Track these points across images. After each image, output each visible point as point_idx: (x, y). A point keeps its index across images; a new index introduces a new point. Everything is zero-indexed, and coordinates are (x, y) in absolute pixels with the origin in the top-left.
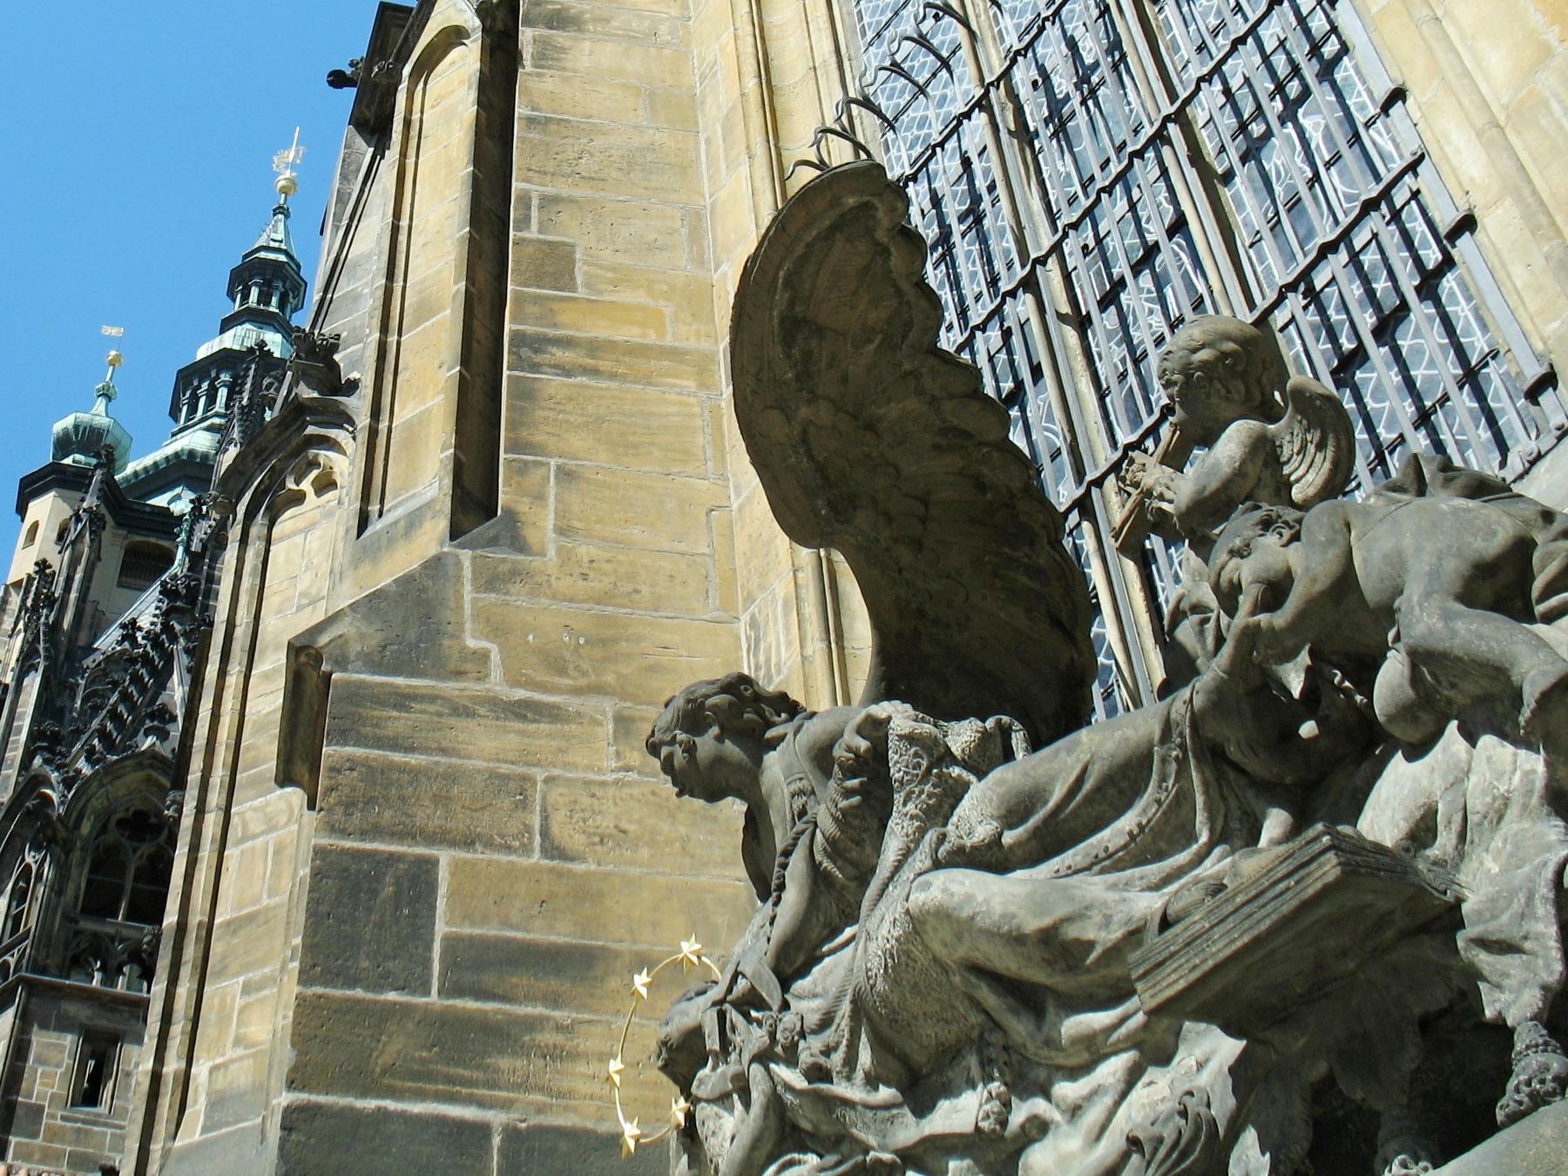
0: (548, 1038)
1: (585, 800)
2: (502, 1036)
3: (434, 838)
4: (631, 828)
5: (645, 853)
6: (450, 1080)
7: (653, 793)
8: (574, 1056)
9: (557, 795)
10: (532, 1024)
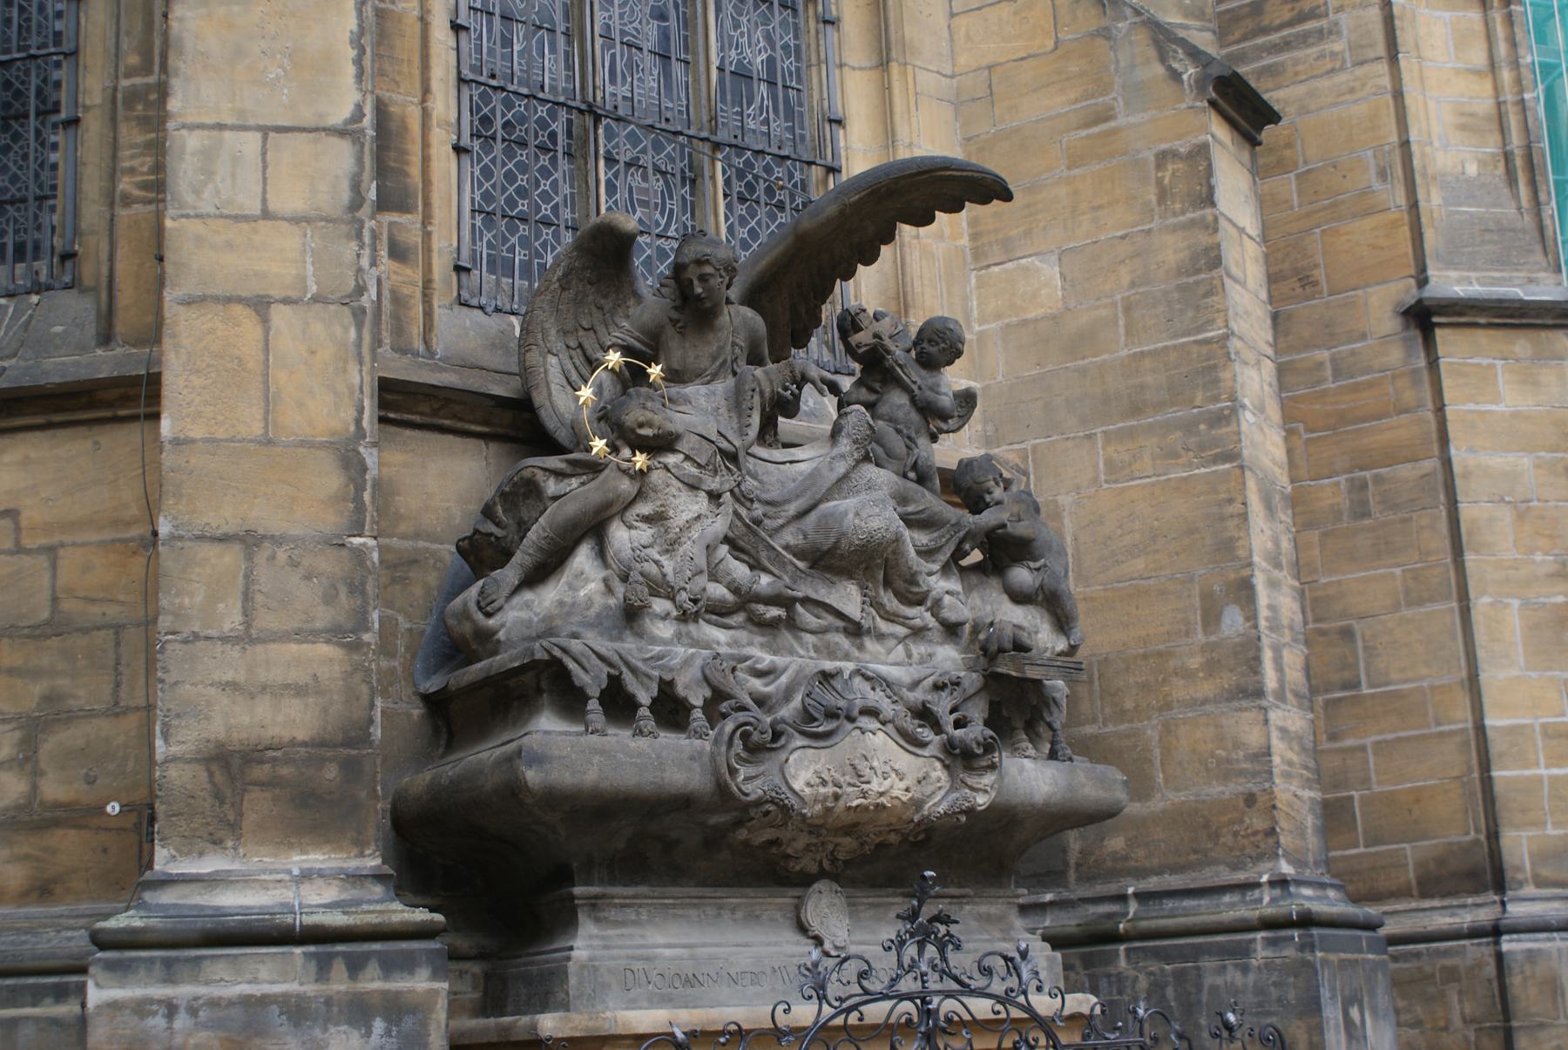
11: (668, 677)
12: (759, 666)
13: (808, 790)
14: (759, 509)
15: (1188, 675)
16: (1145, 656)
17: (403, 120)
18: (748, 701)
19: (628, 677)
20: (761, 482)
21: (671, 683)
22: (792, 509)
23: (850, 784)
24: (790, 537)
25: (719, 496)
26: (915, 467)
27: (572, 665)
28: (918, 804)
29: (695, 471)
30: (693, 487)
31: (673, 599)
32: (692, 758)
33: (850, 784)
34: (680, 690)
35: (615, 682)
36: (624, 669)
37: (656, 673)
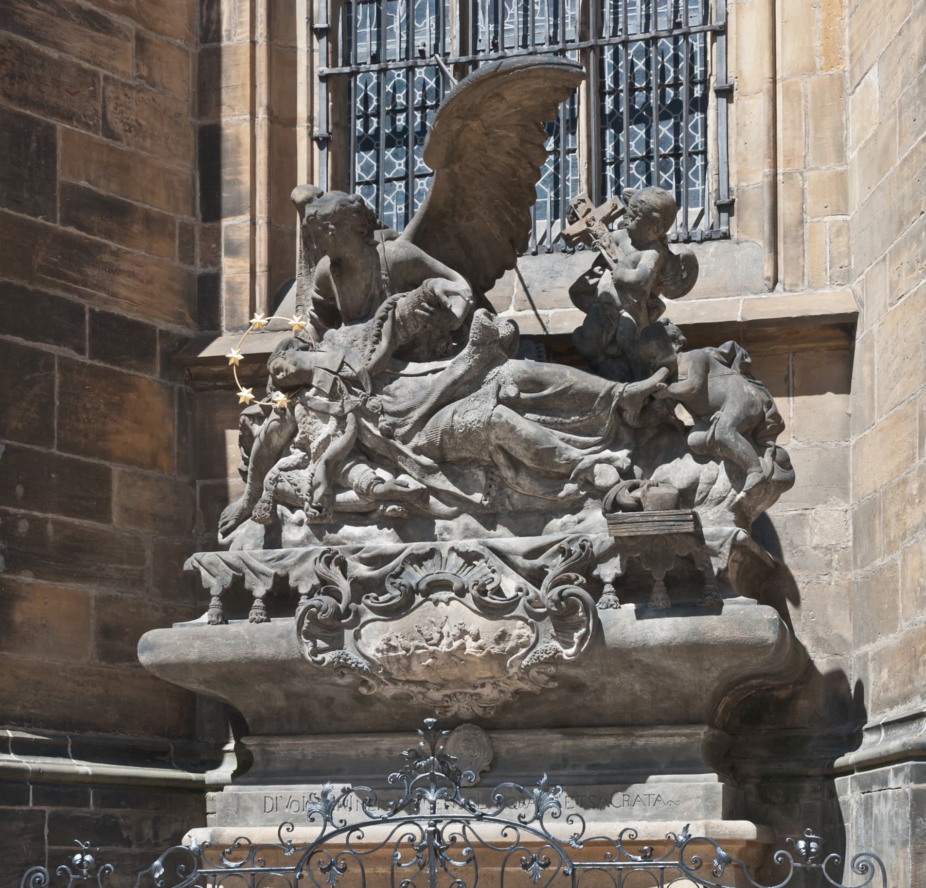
0: (107, 258)
1: (122, 97)
2: (88, 252)
3: (56, 111)
4: (143, 122)
5: (148, 143)
6: (66, 277)
7: (154, 100)
8: (118, 272)
9: (110, 90)
10: (102, 248)
11: (281, 572)
12: (364, 555)
13: (380, 655)
14: (385, 421)
15: (910, 501)
16: (898, 485)
17: (237, 138)
18: (344, 586)
19: (250, 578)
20: (393, 396)
21: (287, 577)
22: (415, 415)
23: (417, 648)
24: (419, 440)
25: (345, 416)
26: (613, 341)
27: (204, 572)
28: (500, 658)
29: (325, 400)
30: (324, 415)
31: (302, 508)
32: (281, 636)
33: (417, 648)
34: (292, 582)
35: (238, 581)
36: (247, 571)
37: (273, 571)
